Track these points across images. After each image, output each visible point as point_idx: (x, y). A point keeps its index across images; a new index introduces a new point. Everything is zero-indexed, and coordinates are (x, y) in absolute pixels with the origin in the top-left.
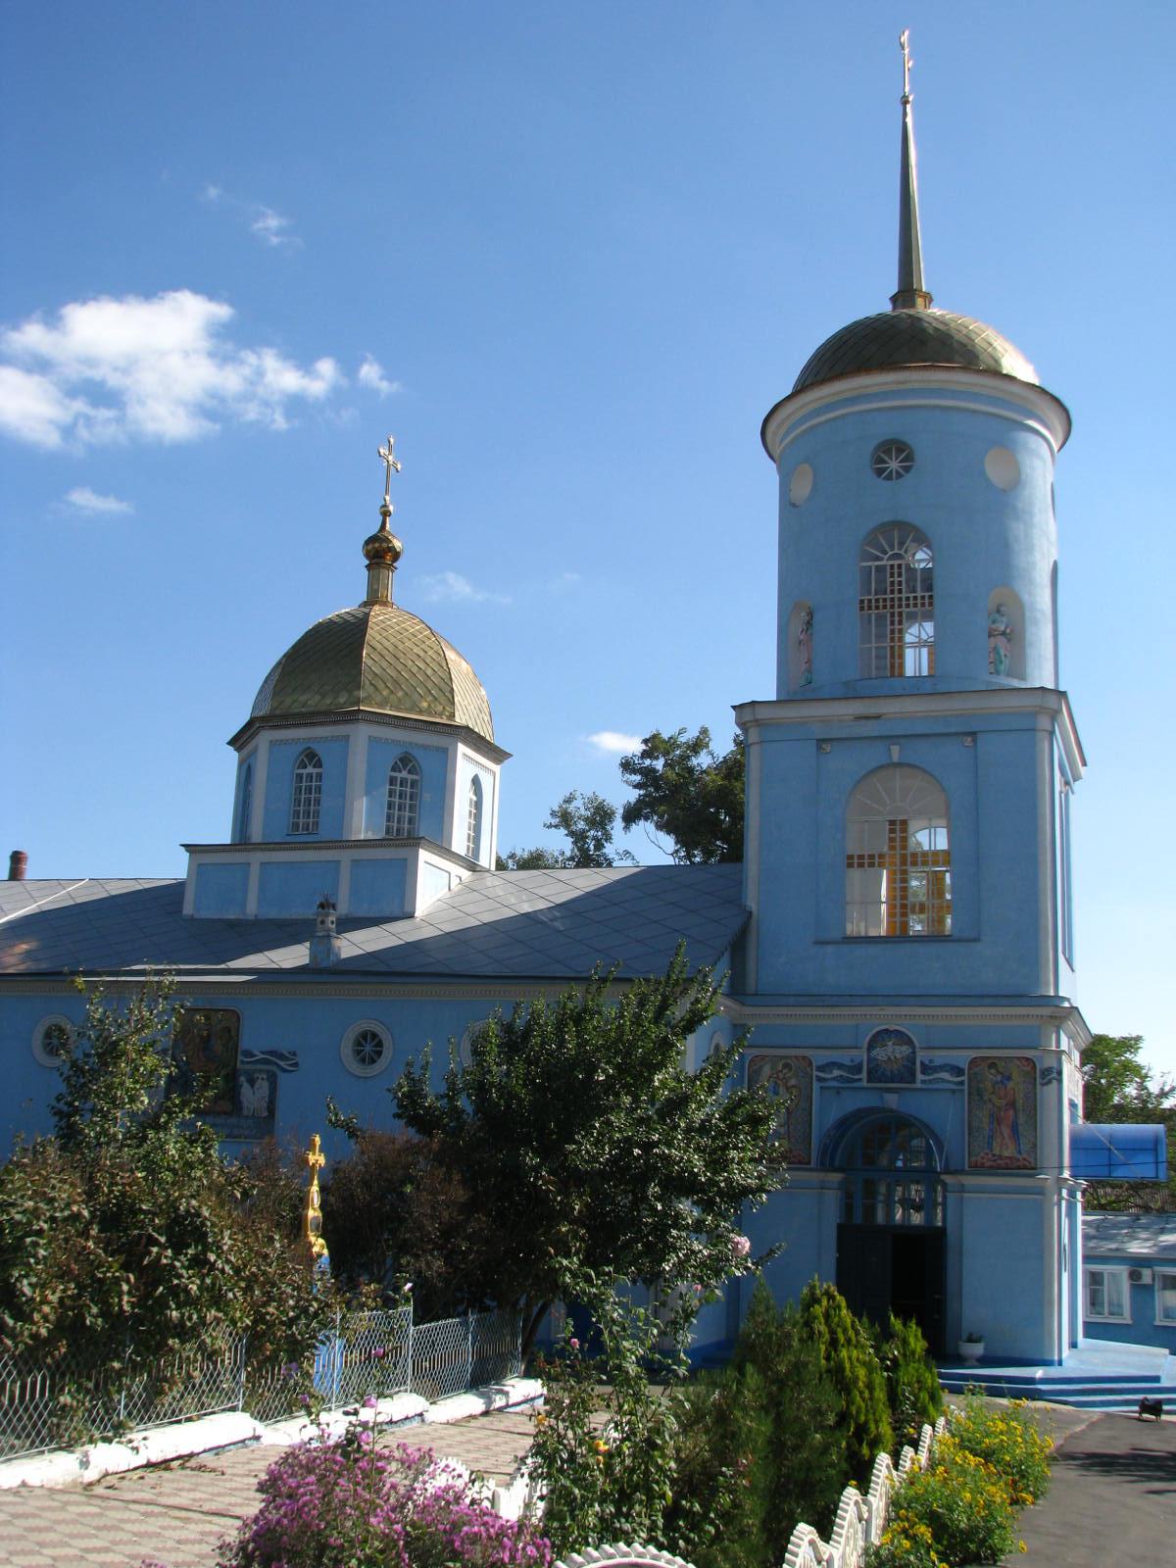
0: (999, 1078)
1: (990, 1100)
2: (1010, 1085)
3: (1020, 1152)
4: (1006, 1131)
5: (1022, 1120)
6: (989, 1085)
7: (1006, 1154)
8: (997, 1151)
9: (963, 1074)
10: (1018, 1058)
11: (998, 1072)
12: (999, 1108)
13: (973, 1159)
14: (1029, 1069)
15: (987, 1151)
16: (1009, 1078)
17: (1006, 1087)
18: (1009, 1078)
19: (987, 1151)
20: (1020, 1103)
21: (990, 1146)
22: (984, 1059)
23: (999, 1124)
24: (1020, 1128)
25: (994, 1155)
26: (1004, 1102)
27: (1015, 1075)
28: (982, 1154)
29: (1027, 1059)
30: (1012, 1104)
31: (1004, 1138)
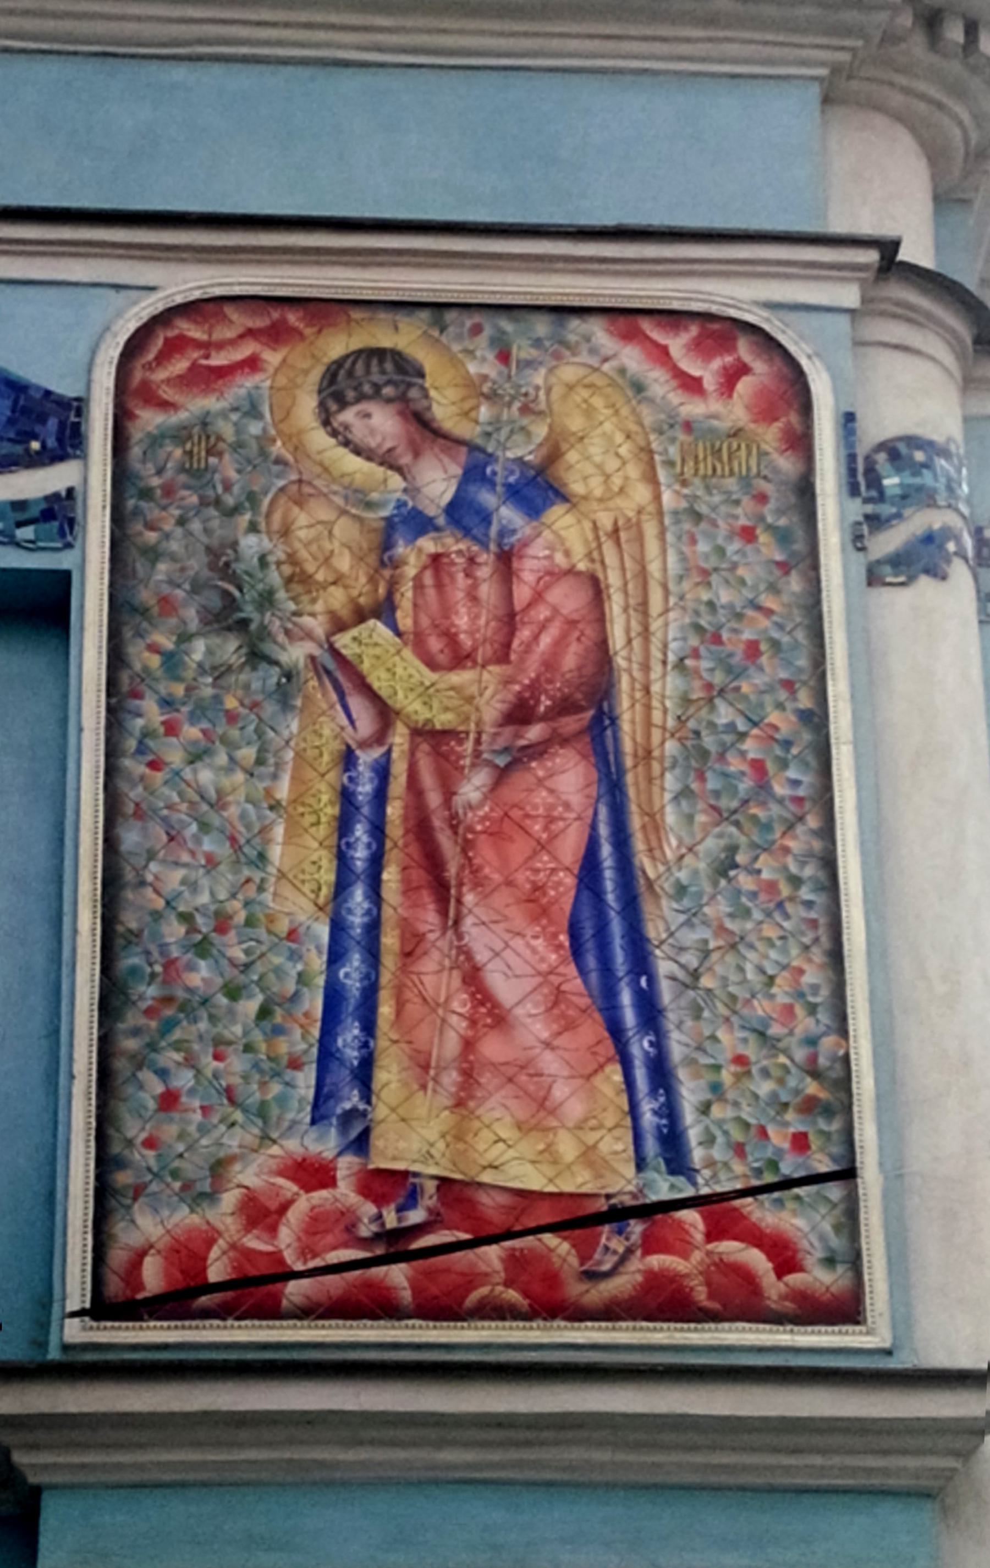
0: (438, 483)
1: (345, 675)
2: (562, 536)
3: (677, 1163)
4: (518, 959)
5: (675, 842)
6: (330, 541)
7: (513, 1162)
8: (413, 1135)
9: (70, 443)
10: (624, 318)
11: (422, 425)
12: (434, 738)
13: (149, 1227)
14: (735, 411)
15: (325, 1144)
16: (539, 488)
17: (507, 560)
18: (539, 488)
19: (325, 1144)
20: (649, 700)
21: (344, 1086)
22: (283, 317)
23: (441, 890)
24: (660, 920)
25: (388, 1185)
26: (483, 693)
27: (601, 462)
28: (250, 1175)
29: (718, 331)
30: (586, 708)
31: (489, 1012)
